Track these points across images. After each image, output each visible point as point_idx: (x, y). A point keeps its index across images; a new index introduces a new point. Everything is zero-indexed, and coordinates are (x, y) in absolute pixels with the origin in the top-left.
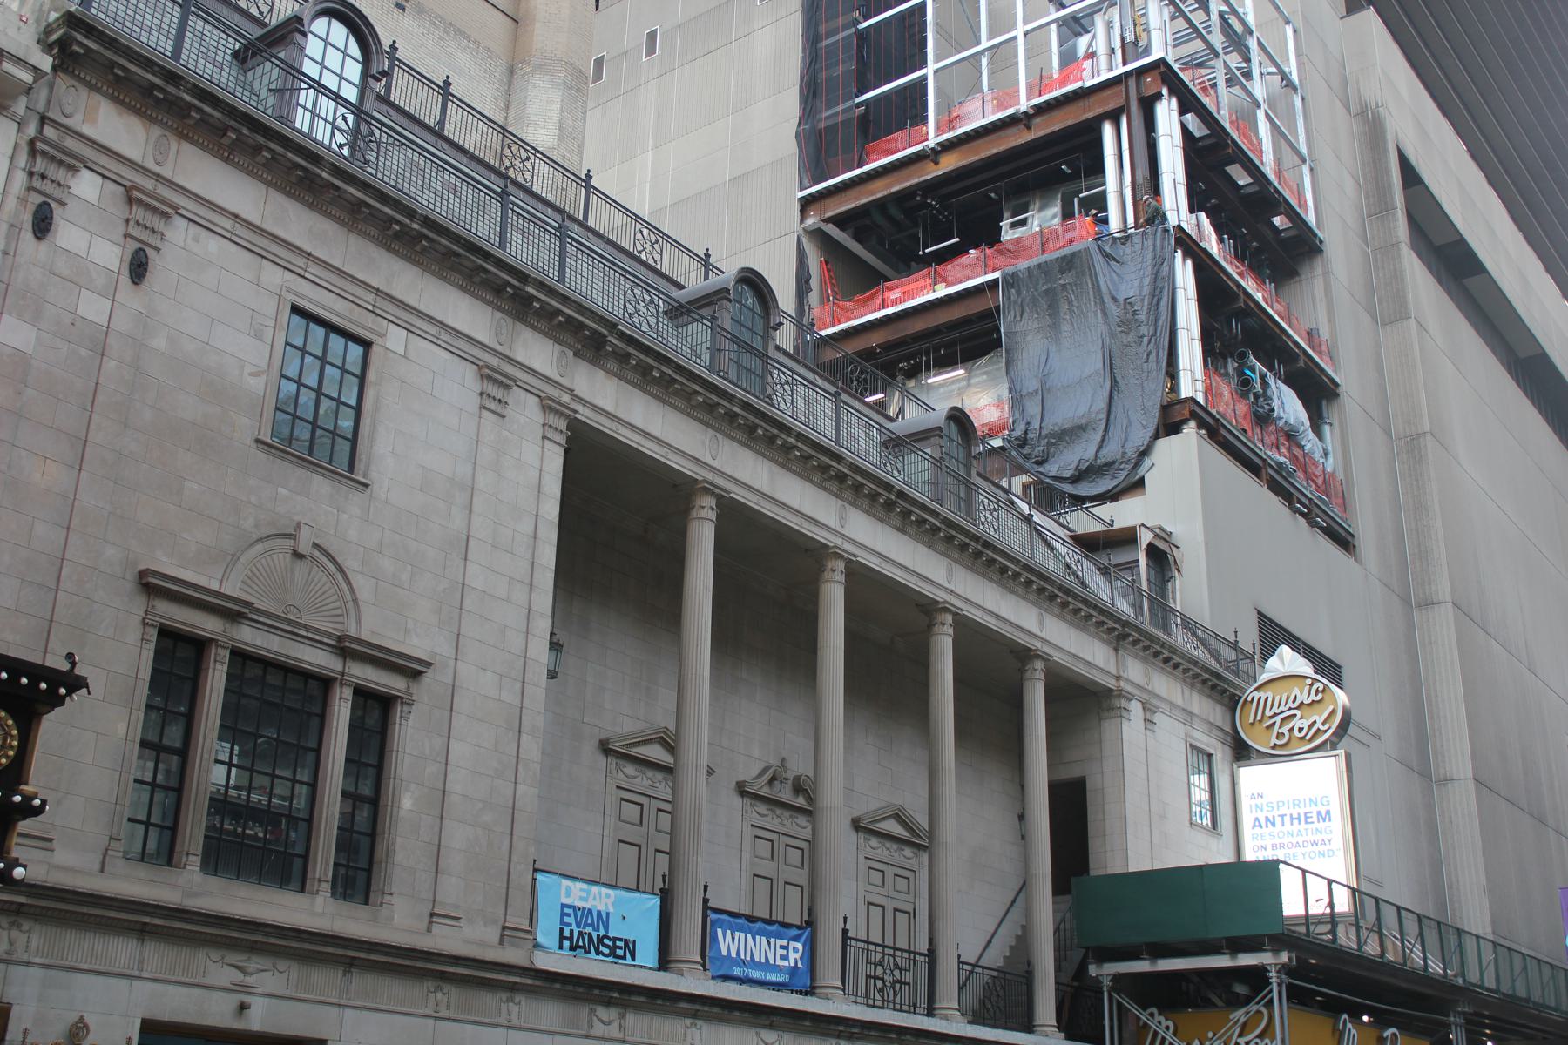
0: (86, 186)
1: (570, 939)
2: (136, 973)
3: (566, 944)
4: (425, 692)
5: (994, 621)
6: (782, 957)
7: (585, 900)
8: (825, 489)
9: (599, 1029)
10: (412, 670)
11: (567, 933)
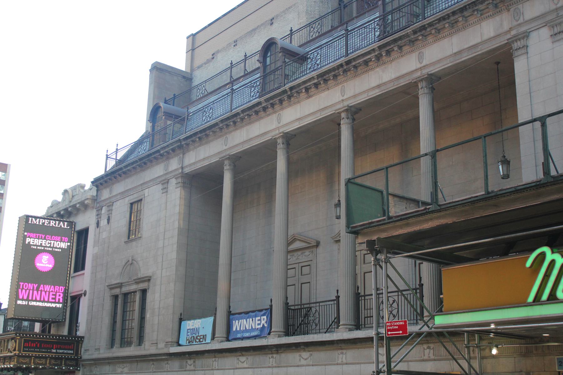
5: (377, 91)
6: (259, 324)
8: (269, 115)
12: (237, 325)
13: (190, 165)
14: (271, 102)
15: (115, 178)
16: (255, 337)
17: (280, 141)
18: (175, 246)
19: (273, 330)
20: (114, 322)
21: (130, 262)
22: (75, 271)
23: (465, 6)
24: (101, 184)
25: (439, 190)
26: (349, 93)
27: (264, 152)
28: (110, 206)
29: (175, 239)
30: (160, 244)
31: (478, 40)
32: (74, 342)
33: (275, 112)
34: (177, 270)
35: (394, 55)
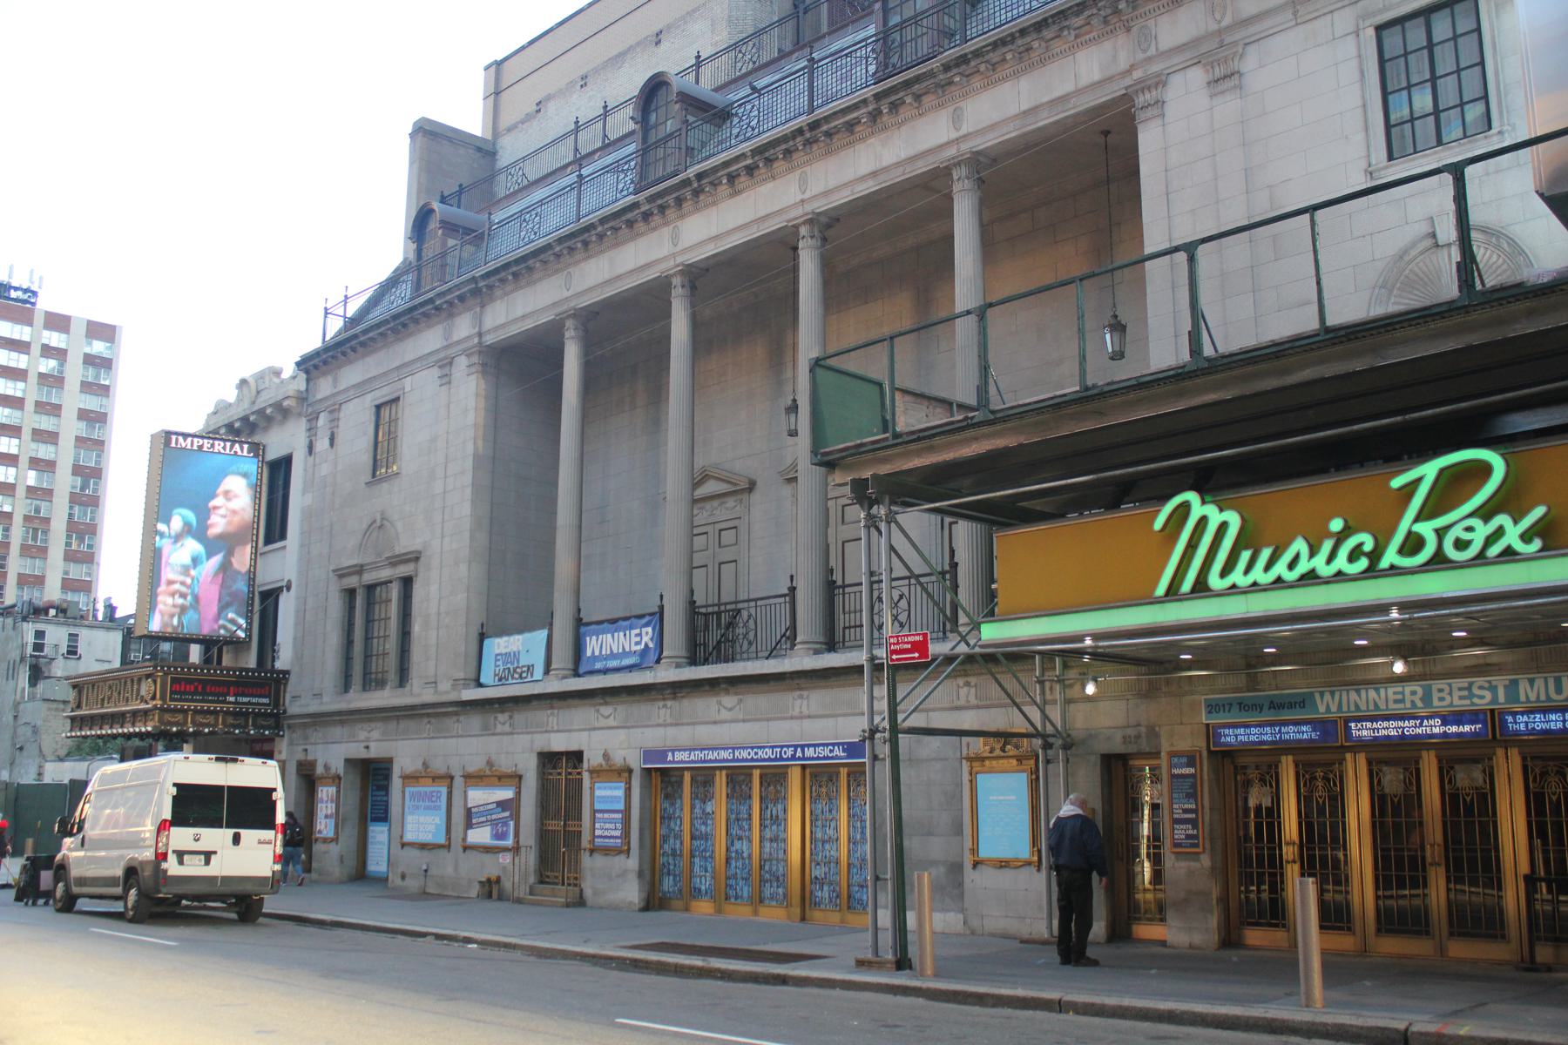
0: (322, 420)
6: (637, 643)
8: (655, 229)
9: (499, 728)
10: (415, 558)
12: (593, 646)
13: (497, 328)
14: (659, 202)
15: (344, 354)
16: (630, 668)
17: (677, 281)
18: (468, 491)
19: (665, 654)
20: (349, 643)
22: (269, 540)
23: (1045, 20)
24: (316, 367)
25: (991, 381)
26: (815, 188)
27: (646, 303)
28: (334, 411)
29: (468, 479)
30: (438, 487)
31: (1068, 87)
32: (271, 682)
33: (666, 224)
34: (472, 538)
35: (905, 112)
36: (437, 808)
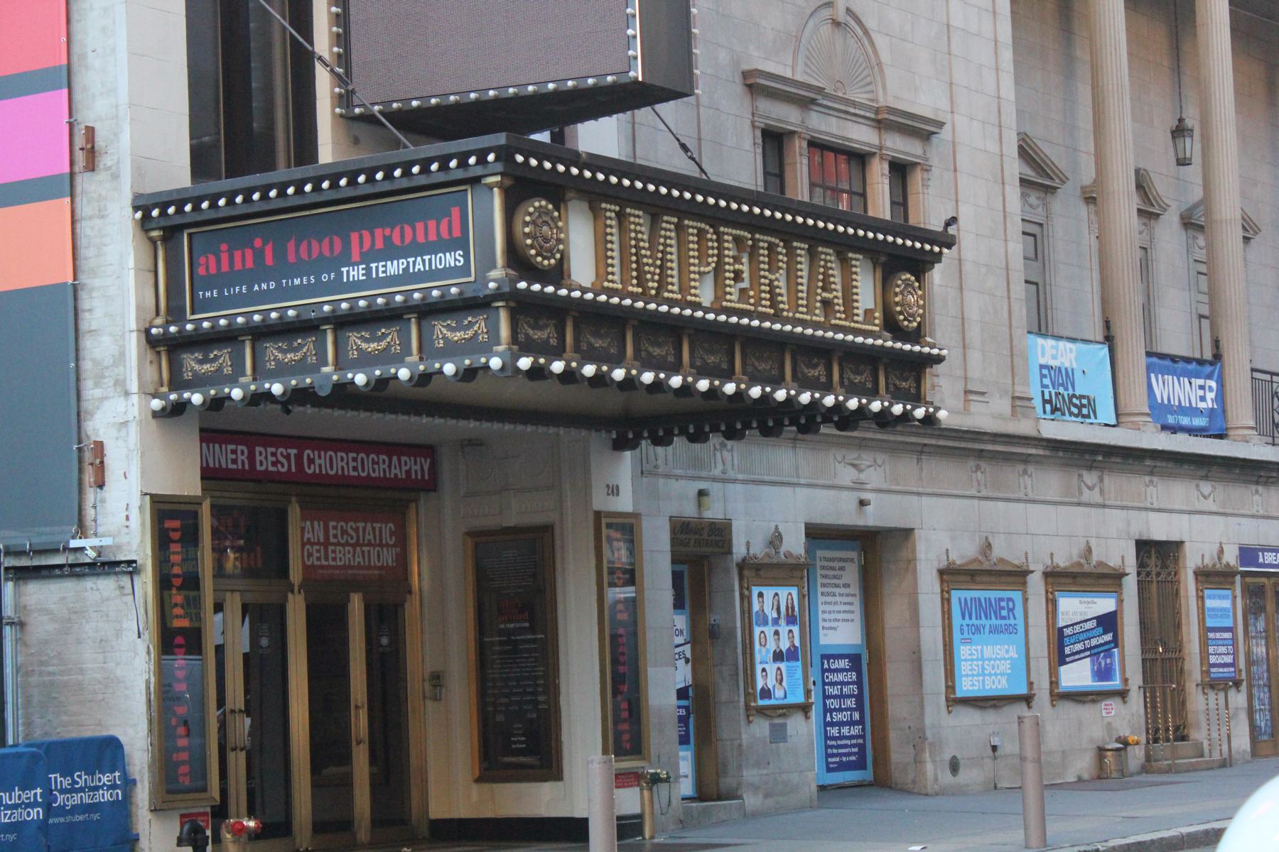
1: (1050, 402)
2: (795, 480)
3: (1048, 407)
4: (936, 153)
7: (1054, 357)
9: (1087, 496)
11: (1047, 397)
21: (841, 16)
36: (1010, 630)
